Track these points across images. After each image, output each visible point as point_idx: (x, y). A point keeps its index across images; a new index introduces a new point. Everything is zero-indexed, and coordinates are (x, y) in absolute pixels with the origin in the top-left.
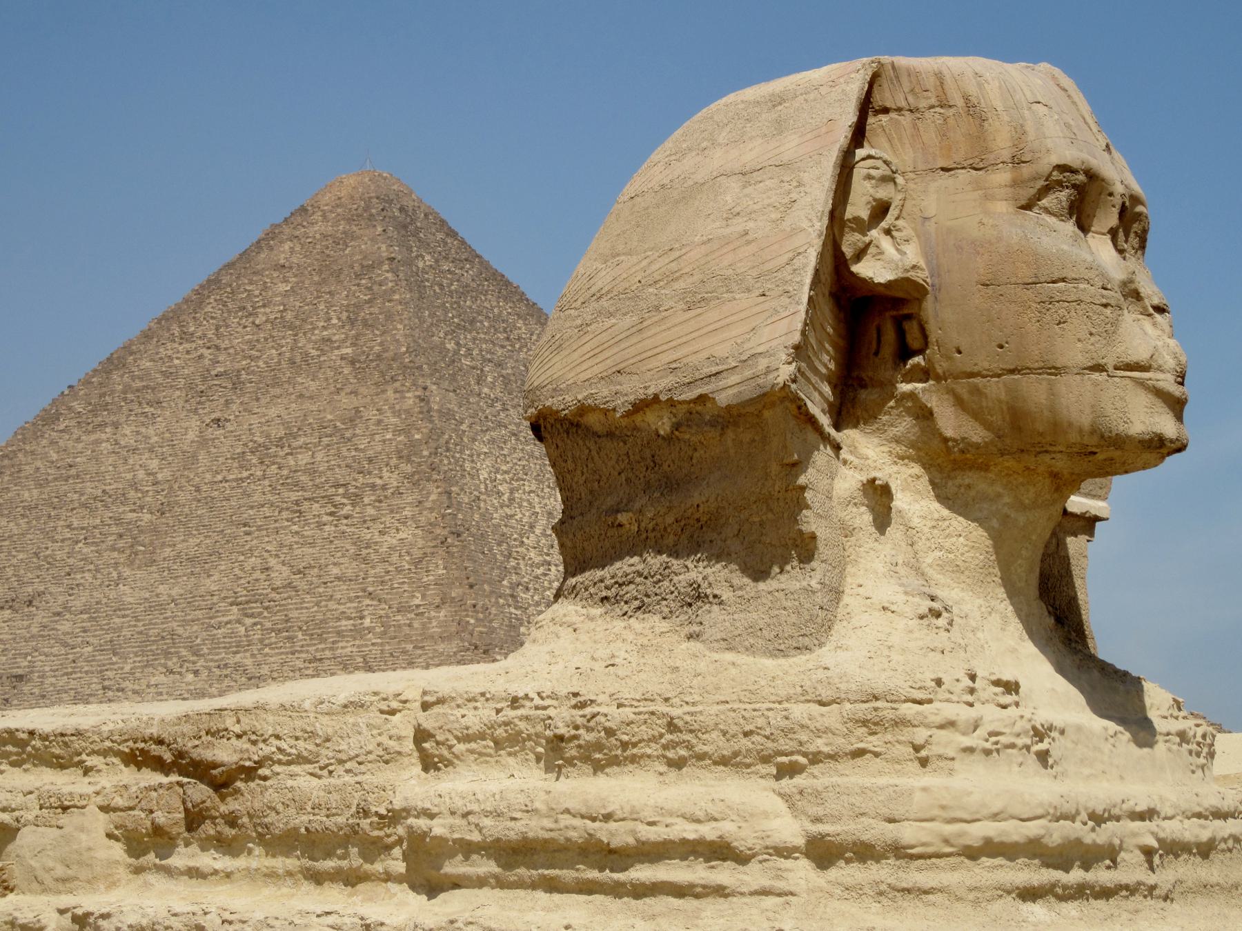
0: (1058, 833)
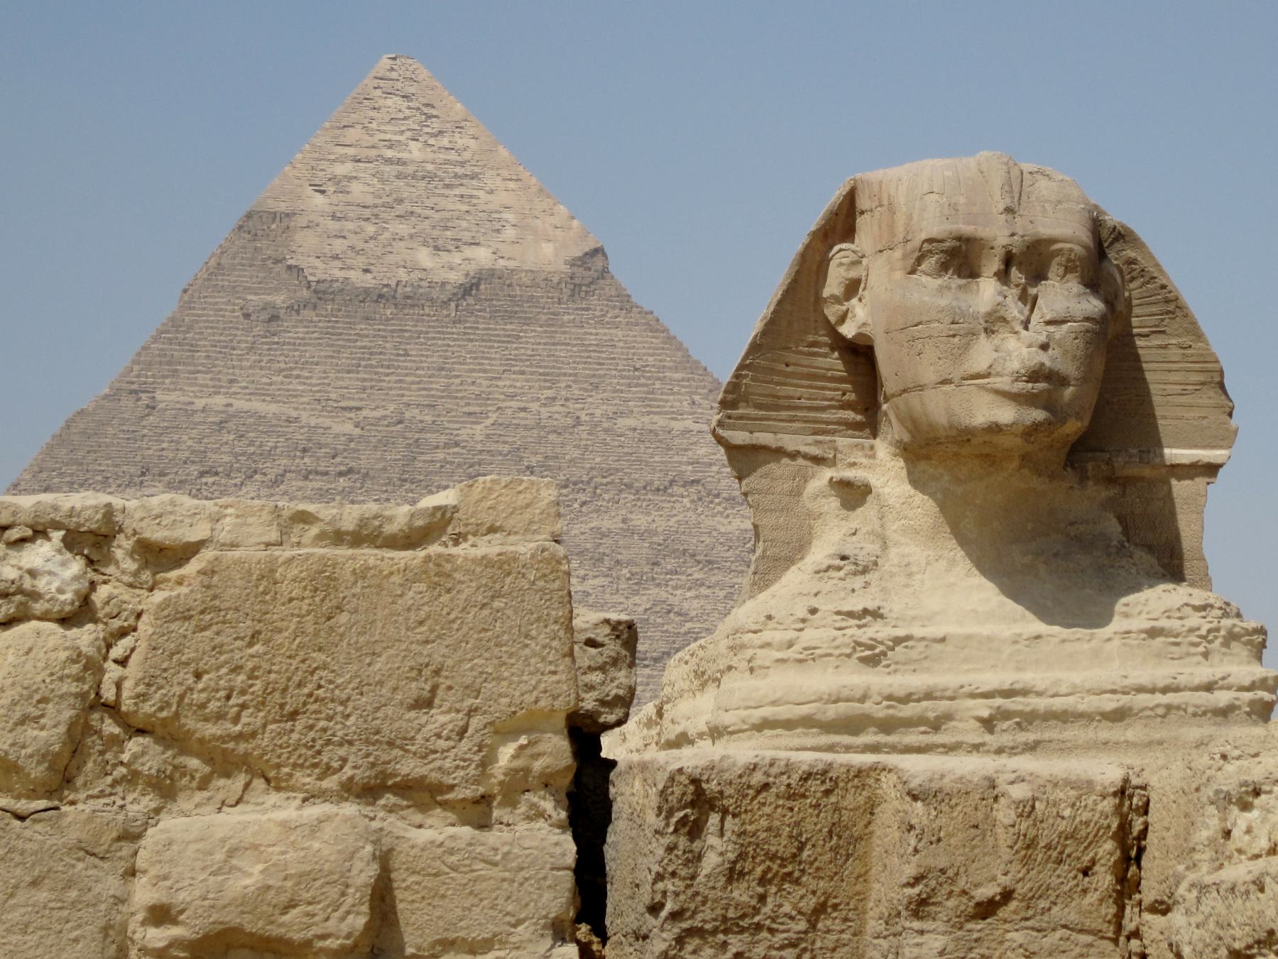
0: (832, 712)
